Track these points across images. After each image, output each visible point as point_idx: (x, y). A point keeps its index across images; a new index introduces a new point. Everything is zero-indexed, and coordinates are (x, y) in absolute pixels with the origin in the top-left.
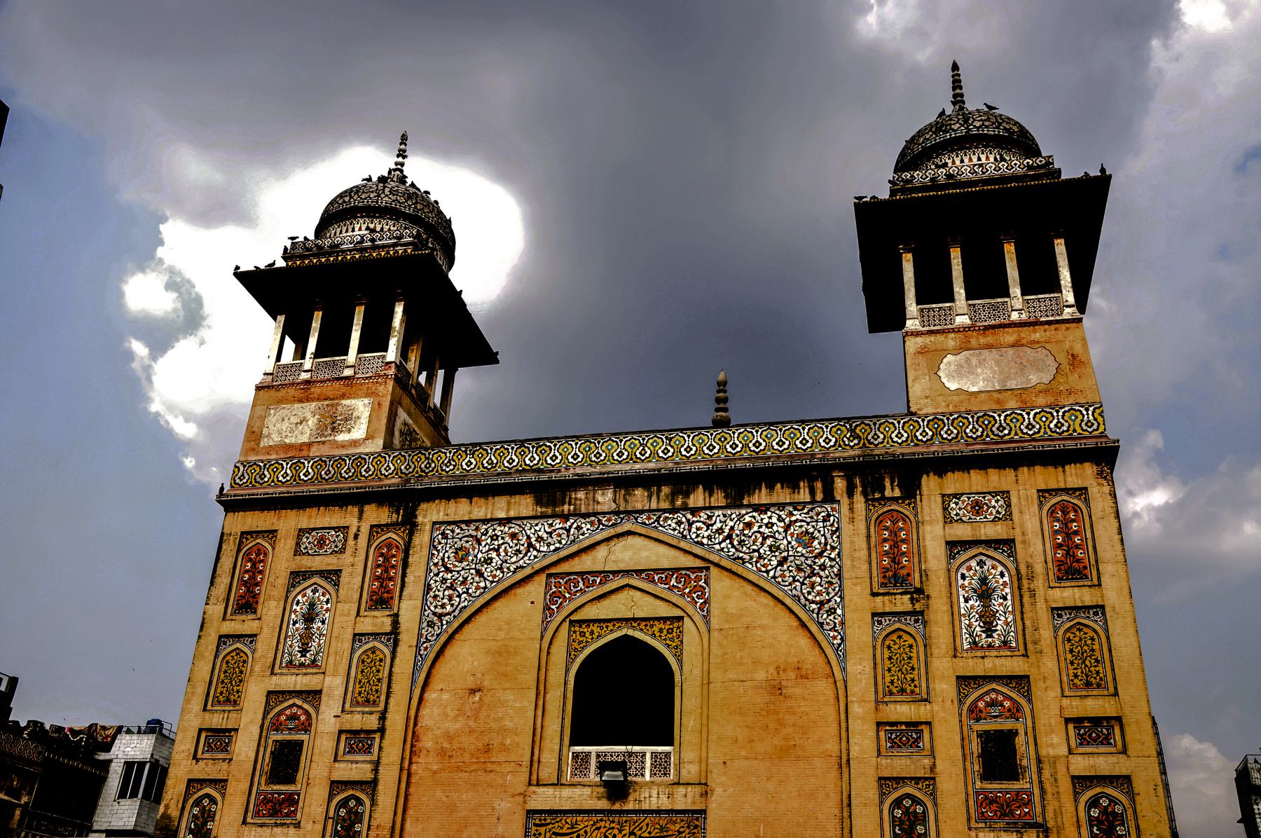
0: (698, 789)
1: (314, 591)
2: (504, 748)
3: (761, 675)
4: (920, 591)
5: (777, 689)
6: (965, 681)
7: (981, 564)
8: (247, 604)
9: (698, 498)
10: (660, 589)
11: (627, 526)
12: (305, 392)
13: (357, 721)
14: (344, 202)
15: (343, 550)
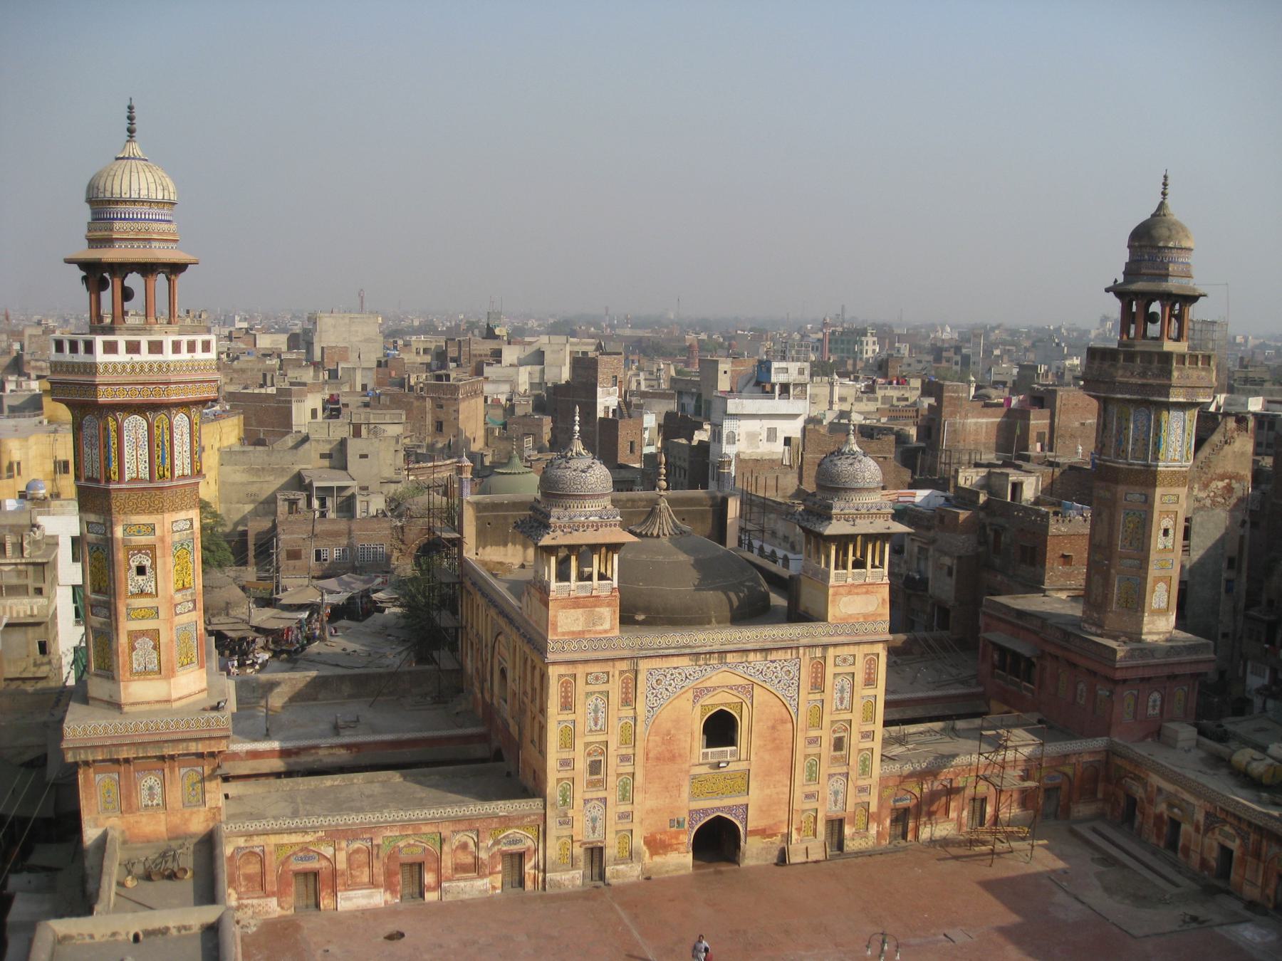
0: (745, 763)
1: (597, 700)
2: (680, 755)
3: (770, 724)
4: (823, 691)
5: (773, 728)
6: (833, 722)
7: (842, 680)
8: (567, 705)
9: (751, 656)
10: (735, 692)
11: (726, 669)
12: (576, 603)
13: (624, 751)
14: (577, 488)
15: (608, 681)
